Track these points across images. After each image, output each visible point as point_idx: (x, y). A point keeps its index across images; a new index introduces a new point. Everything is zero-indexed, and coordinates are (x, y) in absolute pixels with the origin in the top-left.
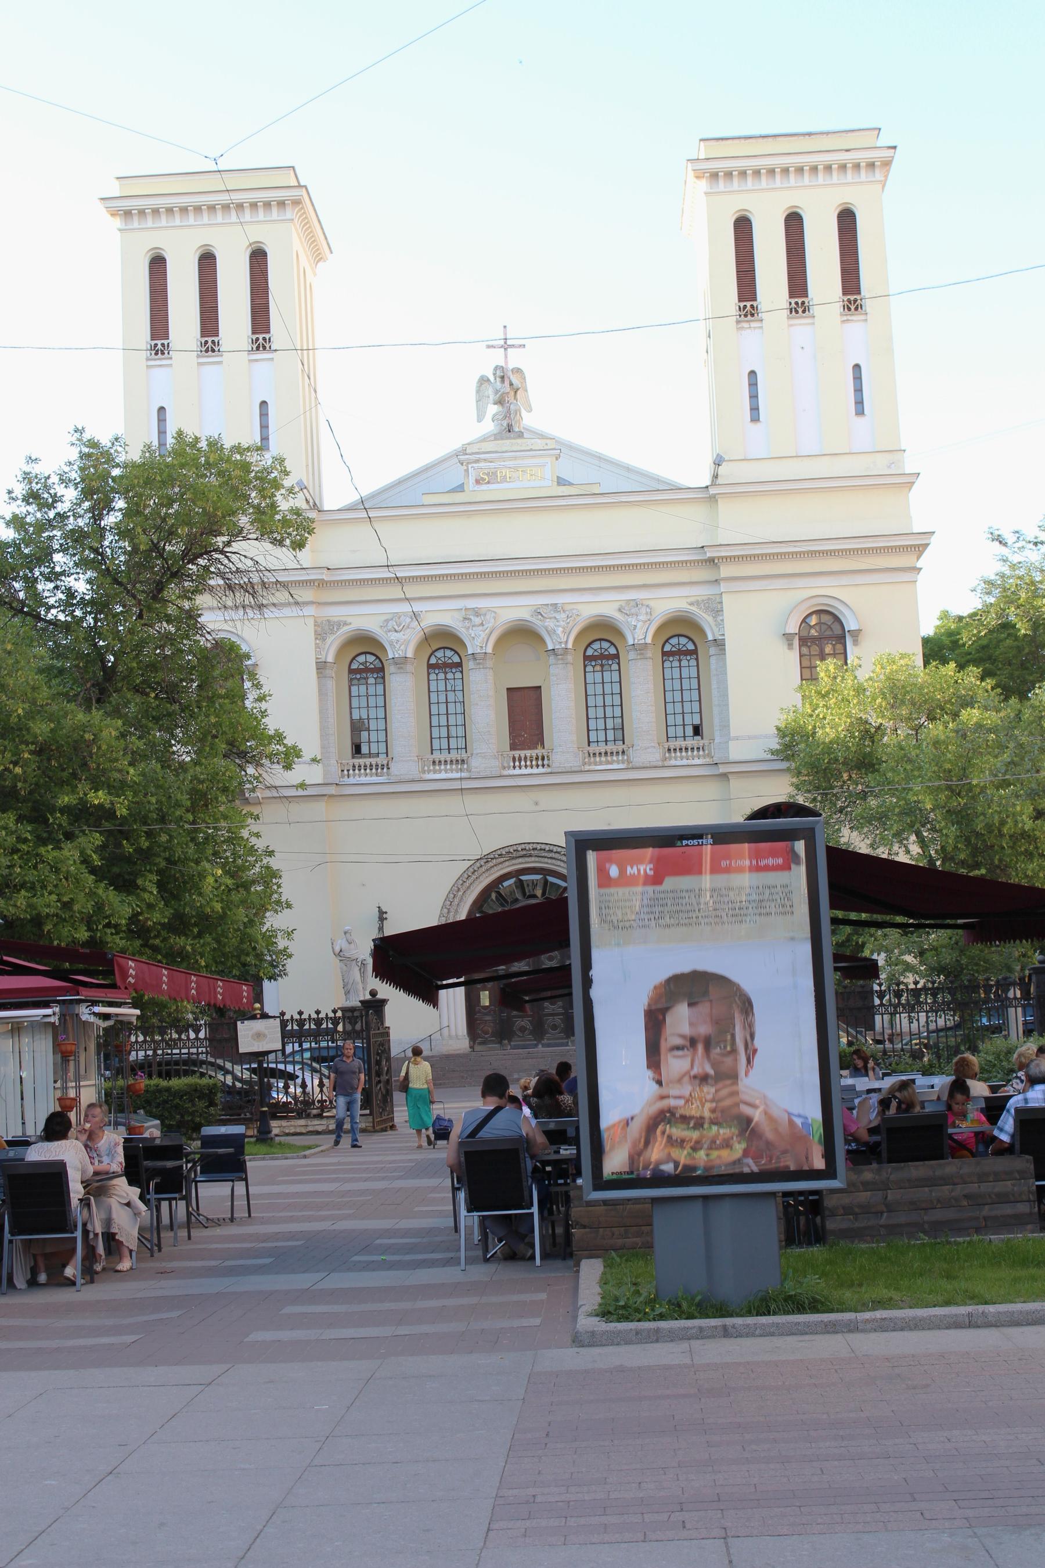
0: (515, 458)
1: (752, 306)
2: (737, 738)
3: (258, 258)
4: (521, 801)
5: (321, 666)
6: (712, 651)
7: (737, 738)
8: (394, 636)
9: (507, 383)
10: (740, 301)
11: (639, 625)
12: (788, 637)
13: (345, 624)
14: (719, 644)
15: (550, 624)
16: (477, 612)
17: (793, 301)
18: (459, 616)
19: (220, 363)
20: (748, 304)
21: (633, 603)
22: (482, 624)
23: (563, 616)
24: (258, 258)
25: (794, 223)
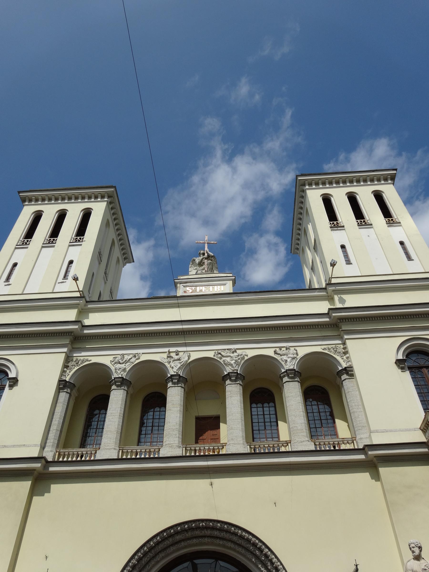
0: (209, 281)
1: (337, 223)
2: (377, 431)
3: (86, 216)
4: (200, 485)
5: (62, 385)
6: (344, 377)
7: (377, 431)
8: (118, 366)
9: (206, 255)
10: (330, 220)
11: (289, 360)
12: (399, 362)
13: (87, 360)
14: (348, 371)
15: (228, 359)
16: (177, 353)
17: (359, 221)
18: (165, 356)
19: (54, 246)
20: (335, 222)
21: (284, 349)
22: (179, 359)
23: (235, 354)
24: (86, 216)
25: (353, 199)
